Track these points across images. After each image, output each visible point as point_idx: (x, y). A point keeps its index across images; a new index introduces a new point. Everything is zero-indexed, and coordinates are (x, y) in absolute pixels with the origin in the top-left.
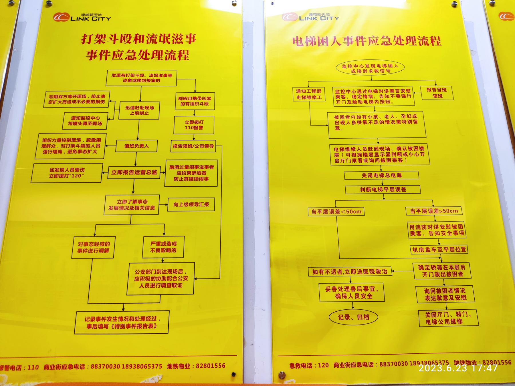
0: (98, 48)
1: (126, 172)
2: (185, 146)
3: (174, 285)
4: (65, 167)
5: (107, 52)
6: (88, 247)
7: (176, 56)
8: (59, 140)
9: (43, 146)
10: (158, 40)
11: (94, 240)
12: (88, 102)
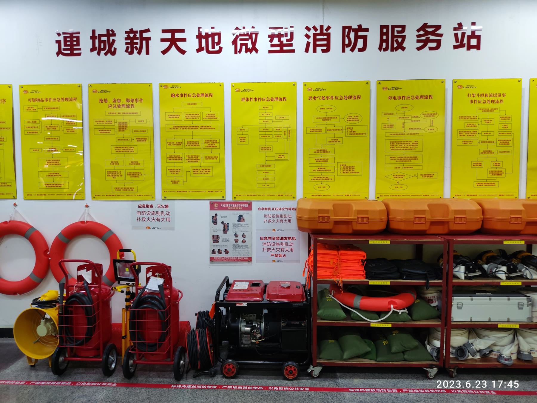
0: (473, 99)
1: (485, 142)
2: (502, 133)
3: (500, 175)
4: (467, 140)
5: (476, 100)
6: (476, 164)
7: (499, 102)
8: (464, 132)
9: (459, 134)
10: (493, 96)
11: (477, 162)
12: (472, 119)
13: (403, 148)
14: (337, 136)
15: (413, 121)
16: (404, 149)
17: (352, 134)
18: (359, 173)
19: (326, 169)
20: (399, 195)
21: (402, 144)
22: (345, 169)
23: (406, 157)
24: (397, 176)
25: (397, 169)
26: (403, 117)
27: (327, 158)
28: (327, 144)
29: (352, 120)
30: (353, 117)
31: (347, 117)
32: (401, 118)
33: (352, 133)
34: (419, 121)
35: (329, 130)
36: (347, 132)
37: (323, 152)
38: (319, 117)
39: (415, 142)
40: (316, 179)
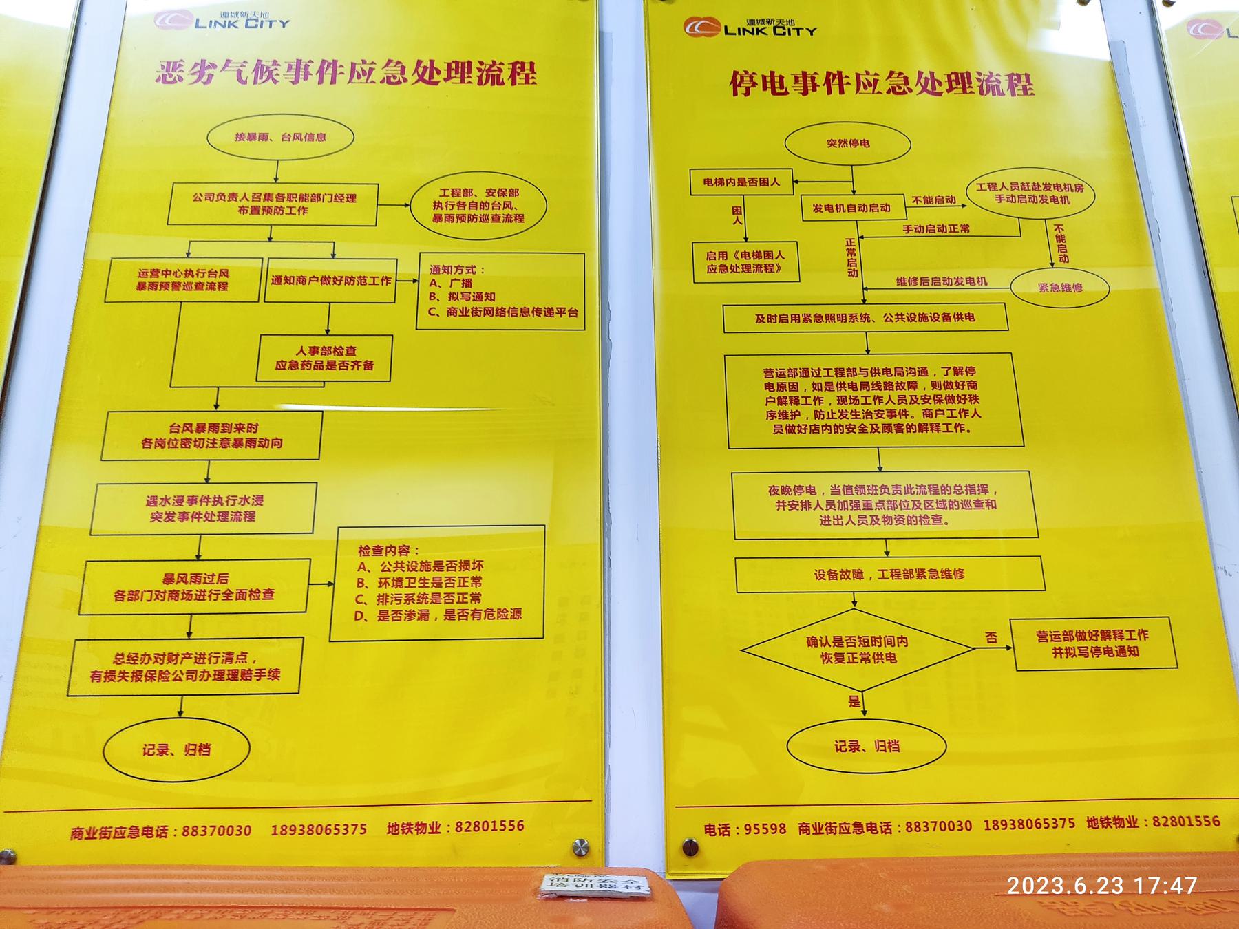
13: (868, 415)
14: (344, 320)
15: (919, 229)
16: (875, 429)
17: (464, 313)
18: (517, 613)
19: (234, 585)
20: (877, 816)
21: (853, 386)
22: (398, 582)
23: (897, 488)
24: (838, 641)
25: (839, 584)
26: (846, 201)
27: (251, 491)
28: (260, 383)
29: (472, 218)
30: (480, 196)
31: (434, 193)
32: (829, 208)
33: (471, 304)
34: (965, 228)
35: (288, 280)
36: (432, 296)
37: (225, 443)
38: (216, 189)
39: (952, 377)
40: (137, 676)
